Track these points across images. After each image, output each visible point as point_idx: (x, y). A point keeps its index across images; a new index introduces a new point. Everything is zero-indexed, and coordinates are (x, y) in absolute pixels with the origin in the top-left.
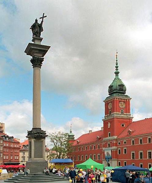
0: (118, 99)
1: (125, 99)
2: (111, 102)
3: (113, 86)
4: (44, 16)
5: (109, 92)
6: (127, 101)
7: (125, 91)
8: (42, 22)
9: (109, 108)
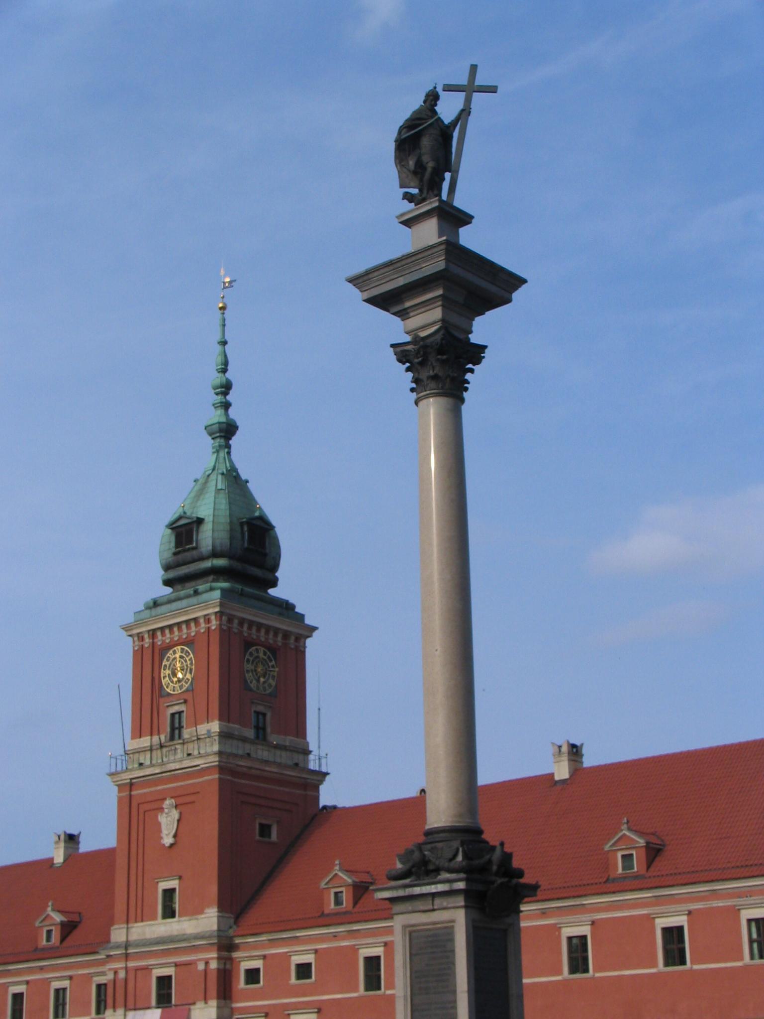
0: (242, 622)
1: (277, 631)
2: (188, 642)
3: (200, 521)
4: (477, 83)
5: (167, 568)
6: (292, 640)
7: (275, 567)
8: (465, 112)
9: (169, 686)
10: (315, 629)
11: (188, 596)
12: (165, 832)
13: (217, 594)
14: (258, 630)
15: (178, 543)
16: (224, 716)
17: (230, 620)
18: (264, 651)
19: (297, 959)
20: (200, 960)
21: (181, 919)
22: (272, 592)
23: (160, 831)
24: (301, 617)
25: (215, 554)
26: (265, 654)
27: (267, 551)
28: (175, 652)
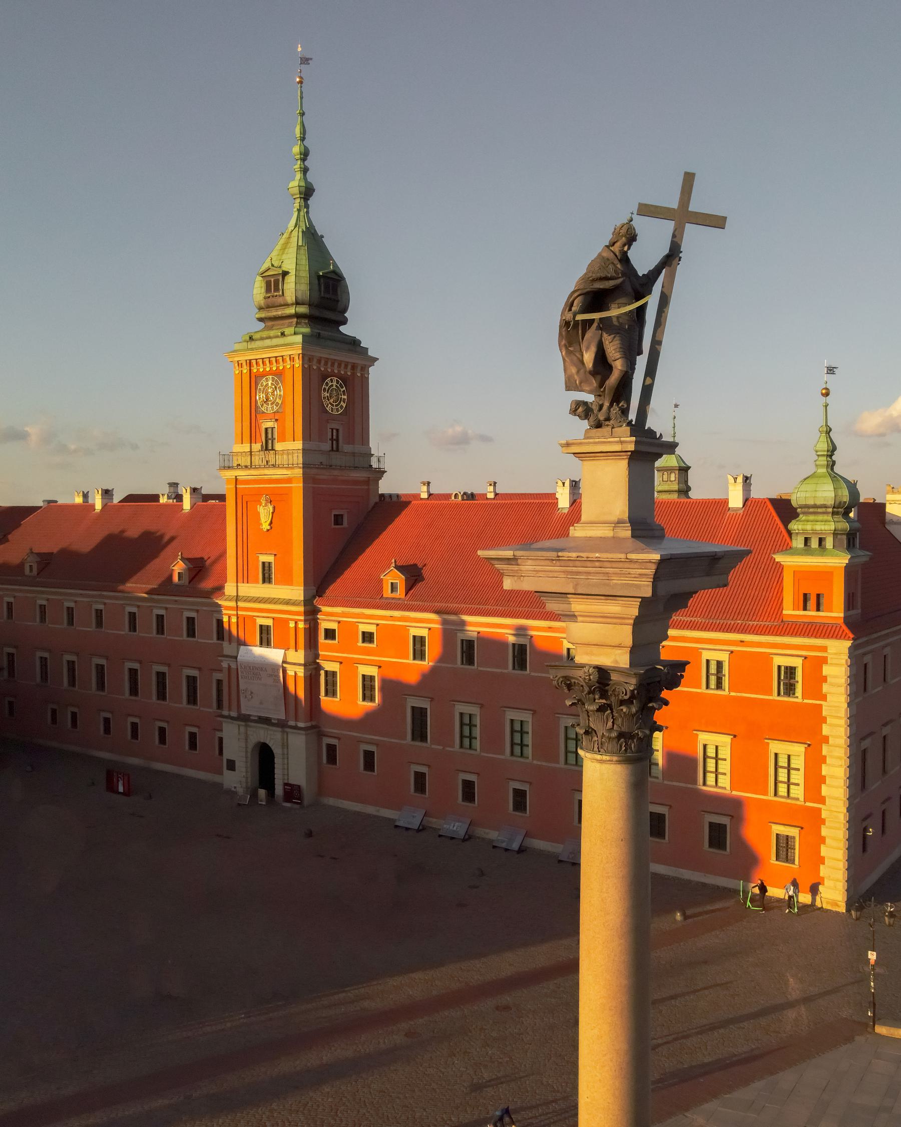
3: (285, 274)
7: (345, 310)
10: (376, 359)
11: (277, 337)
12: (263, 520)
13: (299, 338)
14: (333, 365)
15: (268, 290)
16: (307, 437)
17: (310, 360)
18: (337, 380)
19: (363, 628)
20: (292, 620)
21: (276, 586)
22: (342, 329)
23: (259, 519)
24: (366, 350)
25: (297, 303)
26: (338, 382)
27: (339, 298)
28: (267, 380)
